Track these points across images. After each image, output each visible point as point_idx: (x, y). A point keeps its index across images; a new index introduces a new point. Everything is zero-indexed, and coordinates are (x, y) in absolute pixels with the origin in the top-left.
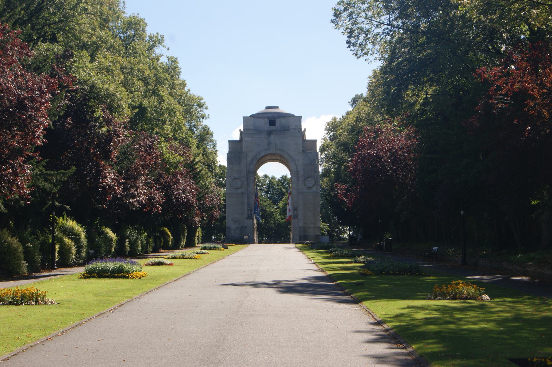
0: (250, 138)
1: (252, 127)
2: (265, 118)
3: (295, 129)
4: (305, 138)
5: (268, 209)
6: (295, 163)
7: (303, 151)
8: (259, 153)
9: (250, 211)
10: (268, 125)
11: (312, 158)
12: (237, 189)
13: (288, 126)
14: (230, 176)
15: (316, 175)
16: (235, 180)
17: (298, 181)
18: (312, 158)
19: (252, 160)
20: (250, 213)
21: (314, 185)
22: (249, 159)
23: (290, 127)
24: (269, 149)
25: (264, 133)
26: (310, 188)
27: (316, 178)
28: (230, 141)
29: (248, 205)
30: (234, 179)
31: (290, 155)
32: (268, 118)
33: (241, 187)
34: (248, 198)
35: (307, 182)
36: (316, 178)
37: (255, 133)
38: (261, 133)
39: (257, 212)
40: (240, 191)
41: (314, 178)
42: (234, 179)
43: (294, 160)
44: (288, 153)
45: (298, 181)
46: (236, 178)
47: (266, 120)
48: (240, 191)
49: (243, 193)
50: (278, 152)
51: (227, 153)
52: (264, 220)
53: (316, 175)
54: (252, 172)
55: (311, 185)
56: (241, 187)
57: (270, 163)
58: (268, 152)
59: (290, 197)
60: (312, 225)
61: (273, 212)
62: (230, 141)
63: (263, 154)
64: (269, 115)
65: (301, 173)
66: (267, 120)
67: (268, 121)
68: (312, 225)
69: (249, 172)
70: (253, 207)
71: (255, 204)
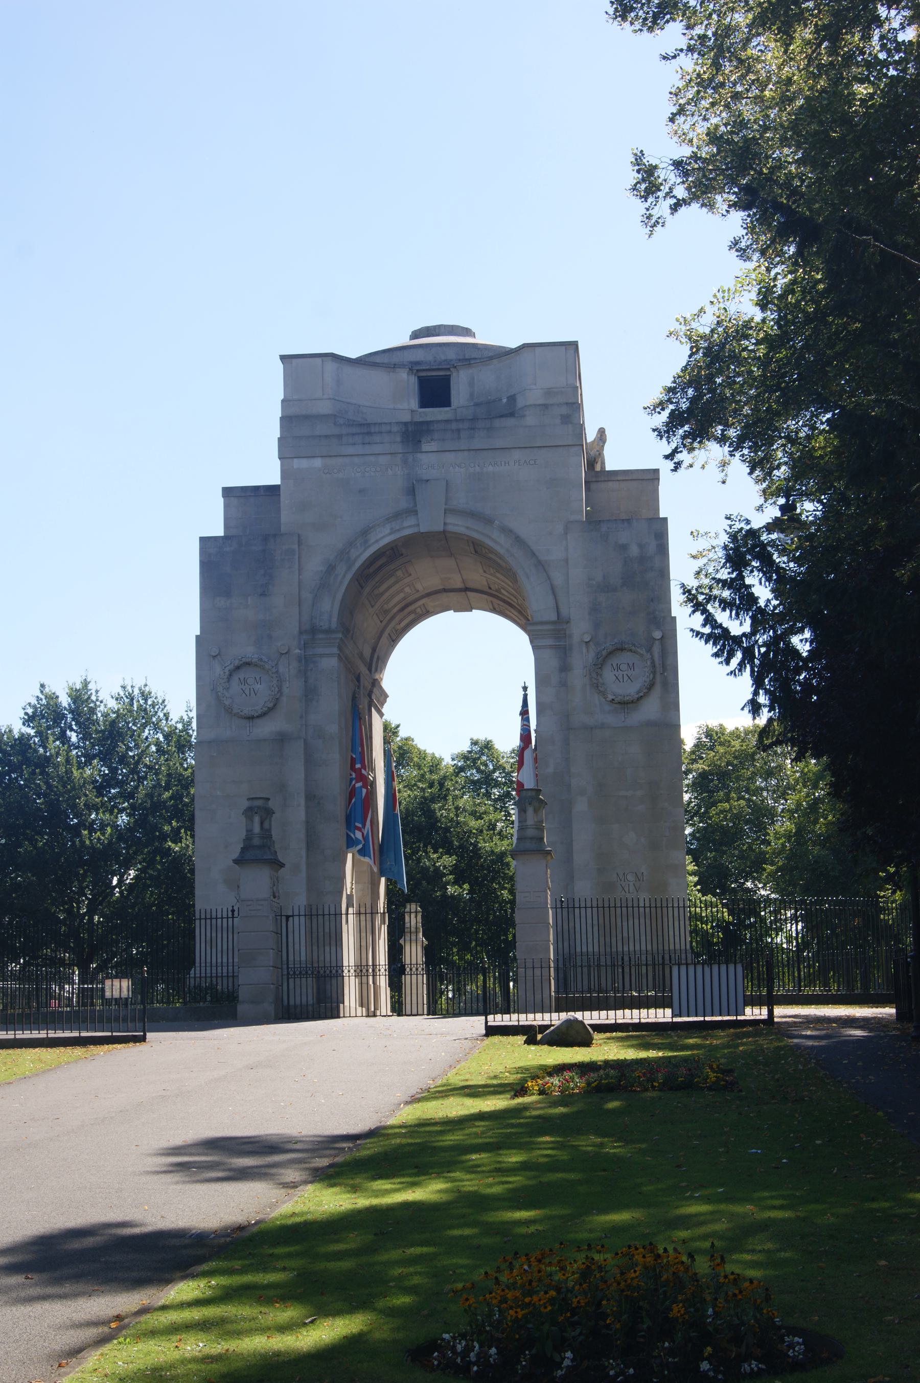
0: (318, 463)
1: (325, 408)
2: (393, 367)
3: (545, 406)
4: (603, 463)
5: (485, 846)
6: (549, 578)
7: (593, 522)
8: (365, 532)
9: (257, 819)
10: (414, 403)
11: (634, 551)
12: (251, 718)
13: (512, 399)
14: (214, 651)
15: (657, 634)
16: (241, 675)
19: (331, 568)
20: (257, 829)
21: (651, 686)
22: (314, 565)
23: (520, 403)
24: (413, 512)
25: (390, 432)
26: (627, 704)
27: (656, 649)
28: (228, 492)
29: (311, 797)
31: (519, 541)
32: (413, 368)
33: (270, 710)
34: (310, 761)
35: (609, 675)
36: (656, 649)
37: (339, 437)
38: (369, 433)
39: (358, 835)
40: (267, 728)
41: (649, 650)
42: (238, 668)
43: (541, 565)
44: (511, 531)
46: (248, 664)
47: (403, 375)
48: (267, 728)
49: (282, 739)
50: (458, 525)
51: (205, 542)
52: (466, 886)
53: (657, 634)
54: (329, 631)
55: (631, 689)
56: (270, 710)
57: (449, 616)
58: (408, 527)
60: (644, 897)
61: (503, 854)
62: (228, 492)
63: (383, 538)
64: (419, 356)
65: (580, 629)
66: (408, 381)
67: (413, 380)
68: (644, 897)
69: (314, 631)
70: (338, 808)
71: (352, 793)
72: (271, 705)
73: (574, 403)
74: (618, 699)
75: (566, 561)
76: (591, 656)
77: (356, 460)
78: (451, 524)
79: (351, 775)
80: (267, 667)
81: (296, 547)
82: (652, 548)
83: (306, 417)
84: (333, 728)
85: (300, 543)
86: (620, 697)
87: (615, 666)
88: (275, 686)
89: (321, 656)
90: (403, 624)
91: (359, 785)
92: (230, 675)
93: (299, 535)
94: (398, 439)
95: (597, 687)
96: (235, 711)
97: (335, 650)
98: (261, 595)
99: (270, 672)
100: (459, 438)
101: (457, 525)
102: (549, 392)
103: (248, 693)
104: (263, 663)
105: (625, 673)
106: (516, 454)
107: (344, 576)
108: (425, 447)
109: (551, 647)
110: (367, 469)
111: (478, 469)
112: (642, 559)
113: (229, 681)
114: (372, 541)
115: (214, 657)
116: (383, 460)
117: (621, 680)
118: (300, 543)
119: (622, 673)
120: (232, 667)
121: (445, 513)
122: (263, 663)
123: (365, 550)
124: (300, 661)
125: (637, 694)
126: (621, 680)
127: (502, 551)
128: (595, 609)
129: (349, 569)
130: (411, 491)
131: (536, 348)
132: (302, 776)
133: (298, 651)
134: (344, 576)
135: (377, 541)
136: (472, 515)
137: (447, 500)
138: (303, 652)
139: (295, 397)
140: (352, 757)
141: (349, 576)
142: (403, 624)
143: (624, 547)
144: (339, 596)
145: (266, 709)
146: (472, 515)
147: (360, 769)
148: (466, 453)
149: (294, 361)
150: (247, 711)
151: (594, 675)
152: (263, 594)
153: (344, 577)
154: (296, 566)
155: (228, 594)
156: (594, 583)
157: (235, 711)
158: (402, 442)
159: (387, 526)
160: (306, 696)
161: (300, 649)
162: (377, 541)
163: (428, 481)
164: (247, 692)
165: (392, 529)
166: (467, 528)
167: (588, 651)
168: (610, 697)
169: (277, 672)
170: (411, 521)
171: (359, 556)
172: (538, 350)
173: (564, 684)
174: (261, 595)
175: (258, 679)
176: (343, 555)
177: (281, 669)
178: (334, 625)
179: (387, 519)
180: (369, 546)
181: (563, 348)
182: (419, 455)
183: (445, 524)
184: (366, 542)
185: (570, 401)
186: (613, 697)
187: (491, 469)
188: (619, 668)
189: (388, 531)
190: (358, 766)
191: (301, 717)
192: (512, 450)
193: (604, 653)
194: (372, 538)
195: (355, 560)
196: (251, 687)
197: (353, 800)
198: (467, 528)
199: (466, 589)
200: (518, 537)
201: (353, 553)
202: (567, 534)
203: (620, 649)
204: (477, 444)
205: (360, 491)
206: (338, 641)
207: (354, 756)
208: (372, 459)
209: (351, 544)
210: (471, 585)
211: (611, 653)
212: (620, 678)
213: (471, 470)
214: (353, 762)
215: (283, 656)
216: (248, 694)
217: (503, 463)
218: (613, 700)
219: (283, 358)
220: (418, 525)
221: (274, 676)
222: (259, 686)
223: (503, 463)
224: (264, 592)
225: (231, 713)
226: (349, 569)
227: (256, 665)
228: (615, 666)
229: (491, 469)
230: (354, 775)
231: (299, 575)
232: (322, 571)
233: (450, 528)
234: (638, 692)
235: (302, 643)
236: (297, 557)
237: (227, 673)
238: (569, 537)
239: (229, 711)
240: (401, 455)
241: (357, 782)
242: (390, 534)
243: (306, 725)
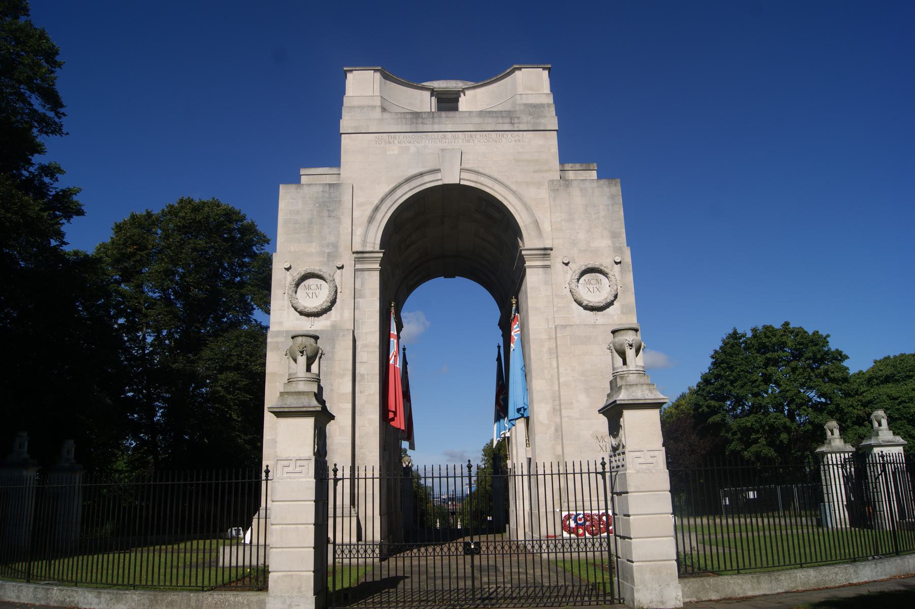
87: (587, 281)
97: (377, 266)
103: (311, 297)
117: (592, 291)
119: (592, 286)
126: (592, 291)
164: (311, 295)
175: (319, 285)
206: (380, 259)
212: (591, 289)
216: (311, 297)
228: (587, 281)
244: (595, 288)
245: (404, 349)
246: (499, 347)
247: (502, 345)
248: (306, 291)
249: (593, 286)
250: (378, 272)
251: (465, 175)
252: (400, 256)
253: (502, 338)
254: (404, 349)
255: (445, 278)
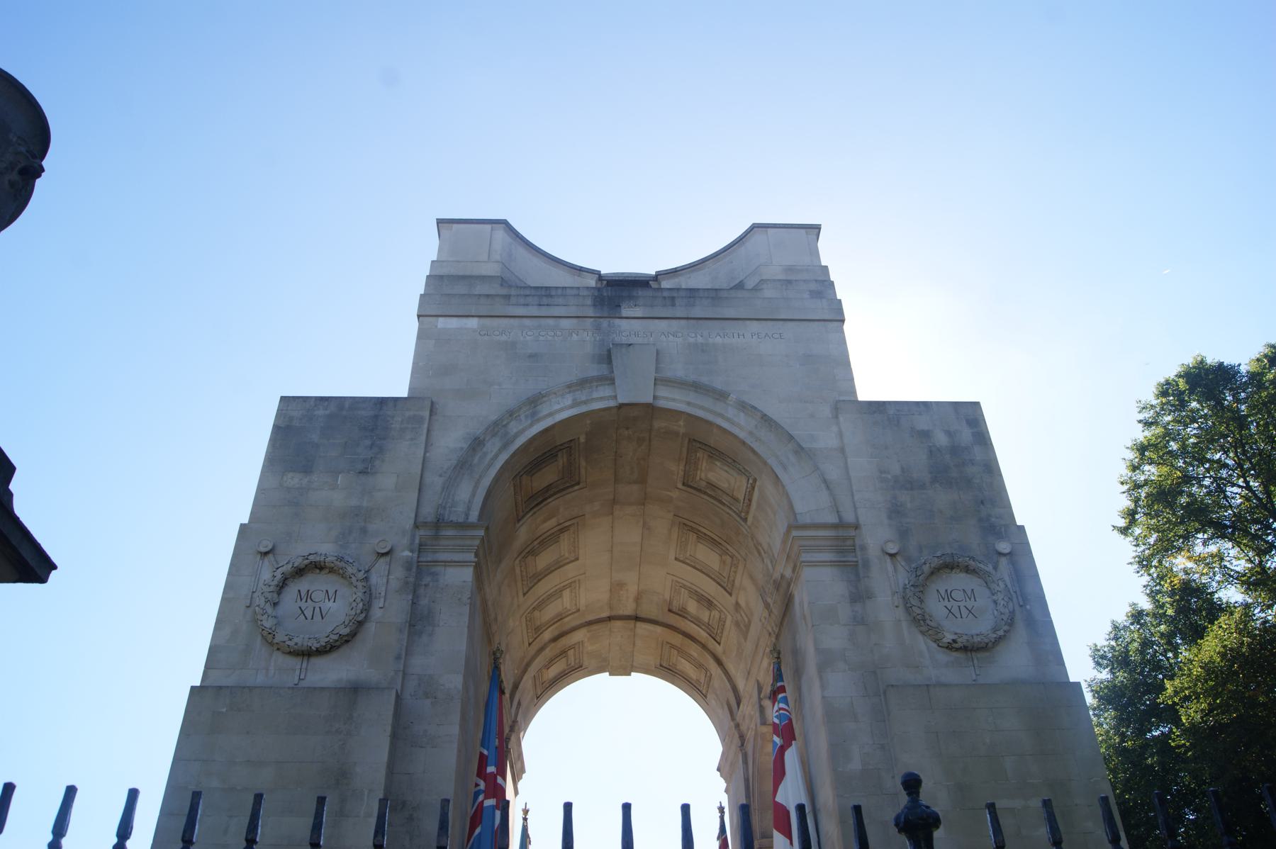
0: (473, 323)
8: (535, 401)
12: (307, 654)
16: (304, 584)
17: (859, 596)
18: (941, 439)
19: (477, 444)
24: (610, 380)
30: (300, 572)
31: (765, 418)
37: (507, 297)
42: (300, 572)
45: (859, 596)
48: (330, 672)
49: (355, 690)
55: (981, 627)
58: (600, 399)
59: (791, 756)
69: (439, 524)
72: (345, 631)
73: (825, 281)
74: (962, 641)
75: (842, 450)
76: (903, 577)
77: (527, 322)
78: (663, 398)
79: (477, 785)
80: (350, 570)
81: (426, 414)
82: (966, 435)
83: (463, 278)
84: (454, 681)
85: (432, 411)
86: (965, 638)
88: (358, 600)
89: (447, 563)
90: (552, 672)
91: (490, 802)
92: (282, 586)
93: (432, 403)
94: (589, 302)
95: (921, 622)
96: (279, 638)
97: (471, 557)
98: (360, 473)
99: (354, 579)
100: (673, 305)
101: (674, 400)
102: (790, 269)
104: (342, 564)
105: (962, 604)
106: (755, 326)
107: (496, 456)
108: (626, 312)
109: (832, 563)
110: (542, 333)
111: (700, 340)
112: (955, 450)
113: (279, 593)
114: (545, 412)
115: (266, 553)
116: (565, 323)
117: (959, 616)
118: (432, 411)
120: (287, 568)
121: (655, 384)
122: (342, 564)
123: (531, 425)
124: (409, 569)
125: (994, 632)
127: (742, 435)
128: (896, 511)
129: (505, 446)
130: (607, 358)
131: (769, 229)
132: (385, 757)
133: (407, 553)
134: (496, 456)
135: (551, 414)
136: (696, 387)
137: (657, 370)
138: (415, 555)
139: (451, 259)
140: (482, 755)
141: (504, 457)
142: (552, 672)
143: (926, 435)
144: (487, 482)
145: (336, 637)
146: (696, 387)
147: (494, 776)
148: (683, 322)
149: (455, 226)
150: (301, 641)
151: (914, 602)
152: (364, 472)
153: (496, 458)
154: (423, 438)
155: (307, 470)
156: (889, 477)
157: (279, 638)
158: (594, 305)
159: (568, 396)
160: (411, 625)
161: (412, 551)
162: (551, 414)
163: (630, 345)
164: (308, 613)
165: (573, 400)
166: (689, 404)
167: (895, 570)
168: (949, 637)
169: (366, 579)
170: (605, 391)
171: (523, 431)
172: (770, 231)
173: (859, 621)
174: (360, 473)
175: (331, 593)
176: (497, 427)
177: (374, 579)
178: (474, 516)
179: (569, 386)
180: (539, 420)
181: (803, 231)
182: (617, 321)
183: (655, 398)
184: (534, 414)
185: (820, 278)
186: (955, 637)
187: (719, 340)
188: (949, 596)
189: (568, 400)
190: (491, 769)
191: (398, 658)
192: (748, 322)
193: (926, 569)
194: (544, 410)
195: (516, 436)
196: (317, 606)
197: (478, 831)
198: (689, 404)
199: (637, 618)
200: (766, 415)
201: (514, 427)
202: (837, 417)
203: (949, 566)
204: (697, 312)
205: (531, 356)
206: (477, 542)
207: (485, 752)
208: (551, 322)
209: (511, 414)
210: (643, 615)
211: (935, 572)
212: (955, 610)
213: (692, 340)
214: (483, 762)
215: (382, 560)
216: (309, 617)
217: (736, 335)
218: (954, 641)
219: (440, 222)
220: (615, 397)
221: (360, 584)
222: (331, 604)
223: (736, 335)
224: (367, 468)
225: (271, 644)
226: (505, 446)
227: (332, 570)
229: (719, 340)
230: (482, 785)
231: (426, 452)
232: (462, 448)
233: (662, 404)
234: (995, 630)
235: (417, 541)
236: (426, 426)
237: (279, 576)
238: (841, 419)
239: (269, 639)
240: (592, 320)
241: (486, 798)
242: (571, 407)
243: (405, 674)
244: (962, 608)
245: (526, 812)
246: (721, 809)
247: (726, 804)
248: (300, 603)
249: (960, 604)
250: (471, 569)
251: (663, 392)
252: (524, 594)
253: (726, 796)
254: (526, 812)
255: (610, 675)
